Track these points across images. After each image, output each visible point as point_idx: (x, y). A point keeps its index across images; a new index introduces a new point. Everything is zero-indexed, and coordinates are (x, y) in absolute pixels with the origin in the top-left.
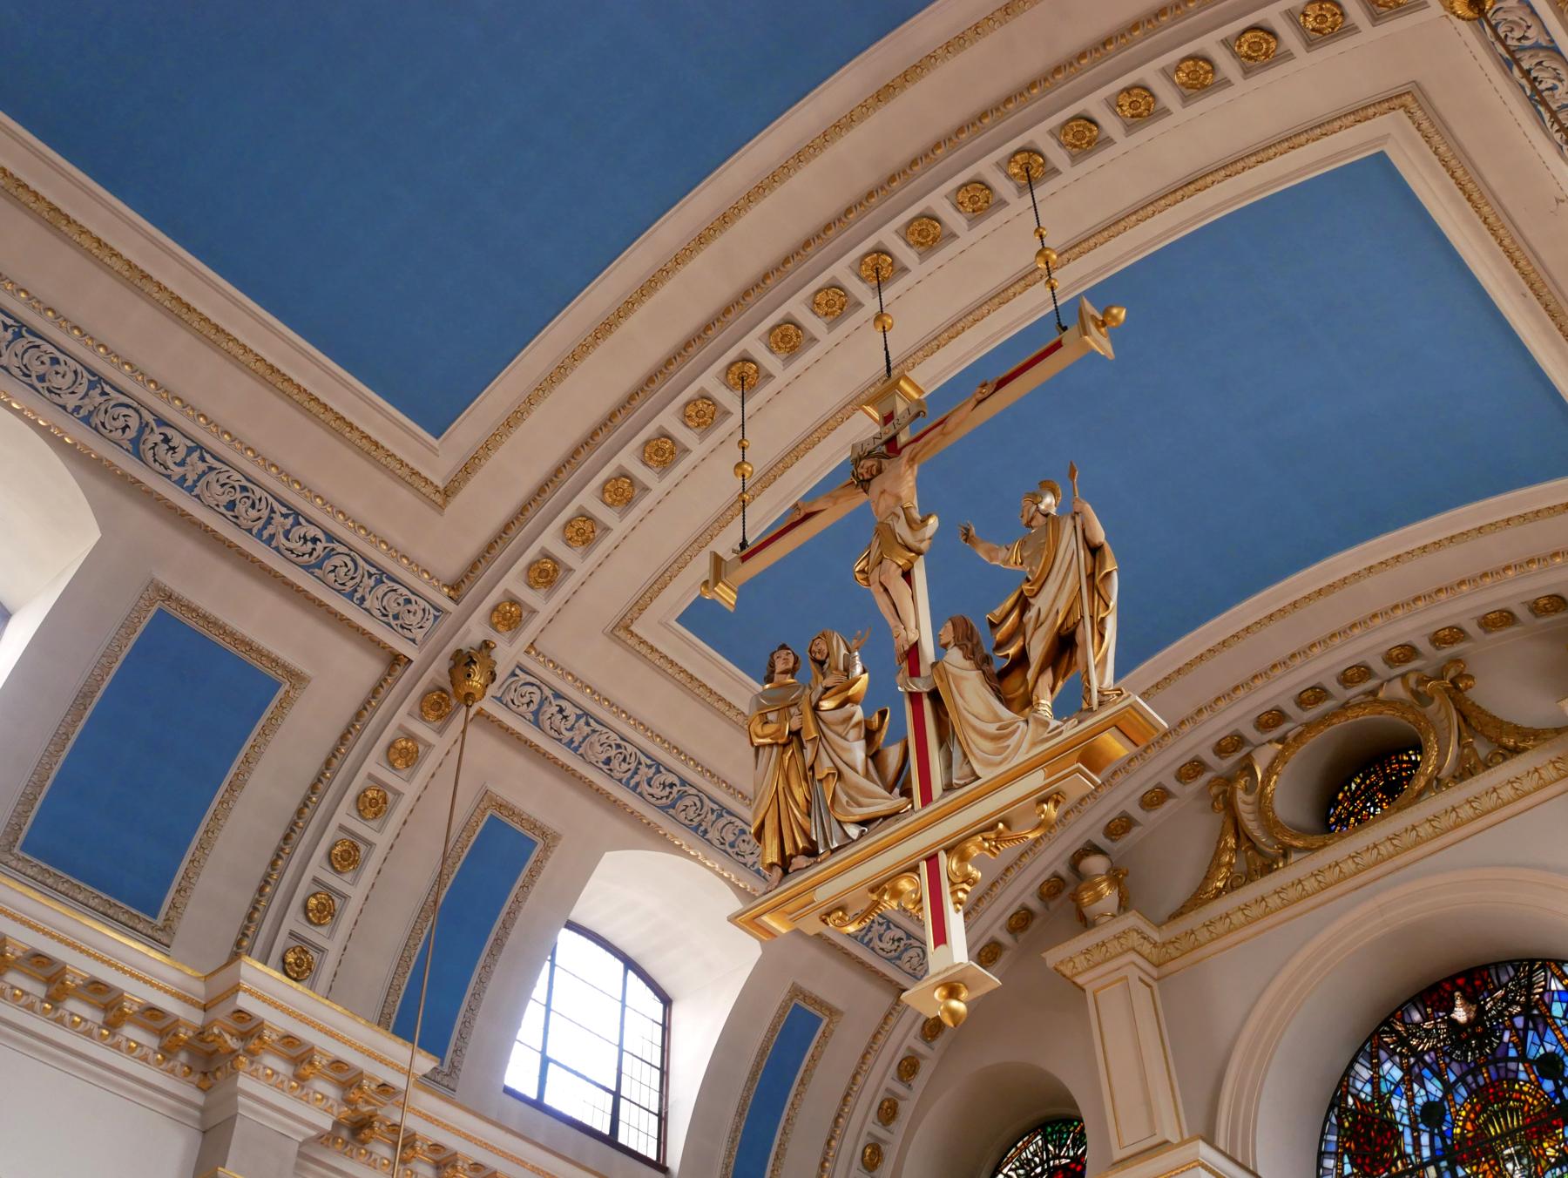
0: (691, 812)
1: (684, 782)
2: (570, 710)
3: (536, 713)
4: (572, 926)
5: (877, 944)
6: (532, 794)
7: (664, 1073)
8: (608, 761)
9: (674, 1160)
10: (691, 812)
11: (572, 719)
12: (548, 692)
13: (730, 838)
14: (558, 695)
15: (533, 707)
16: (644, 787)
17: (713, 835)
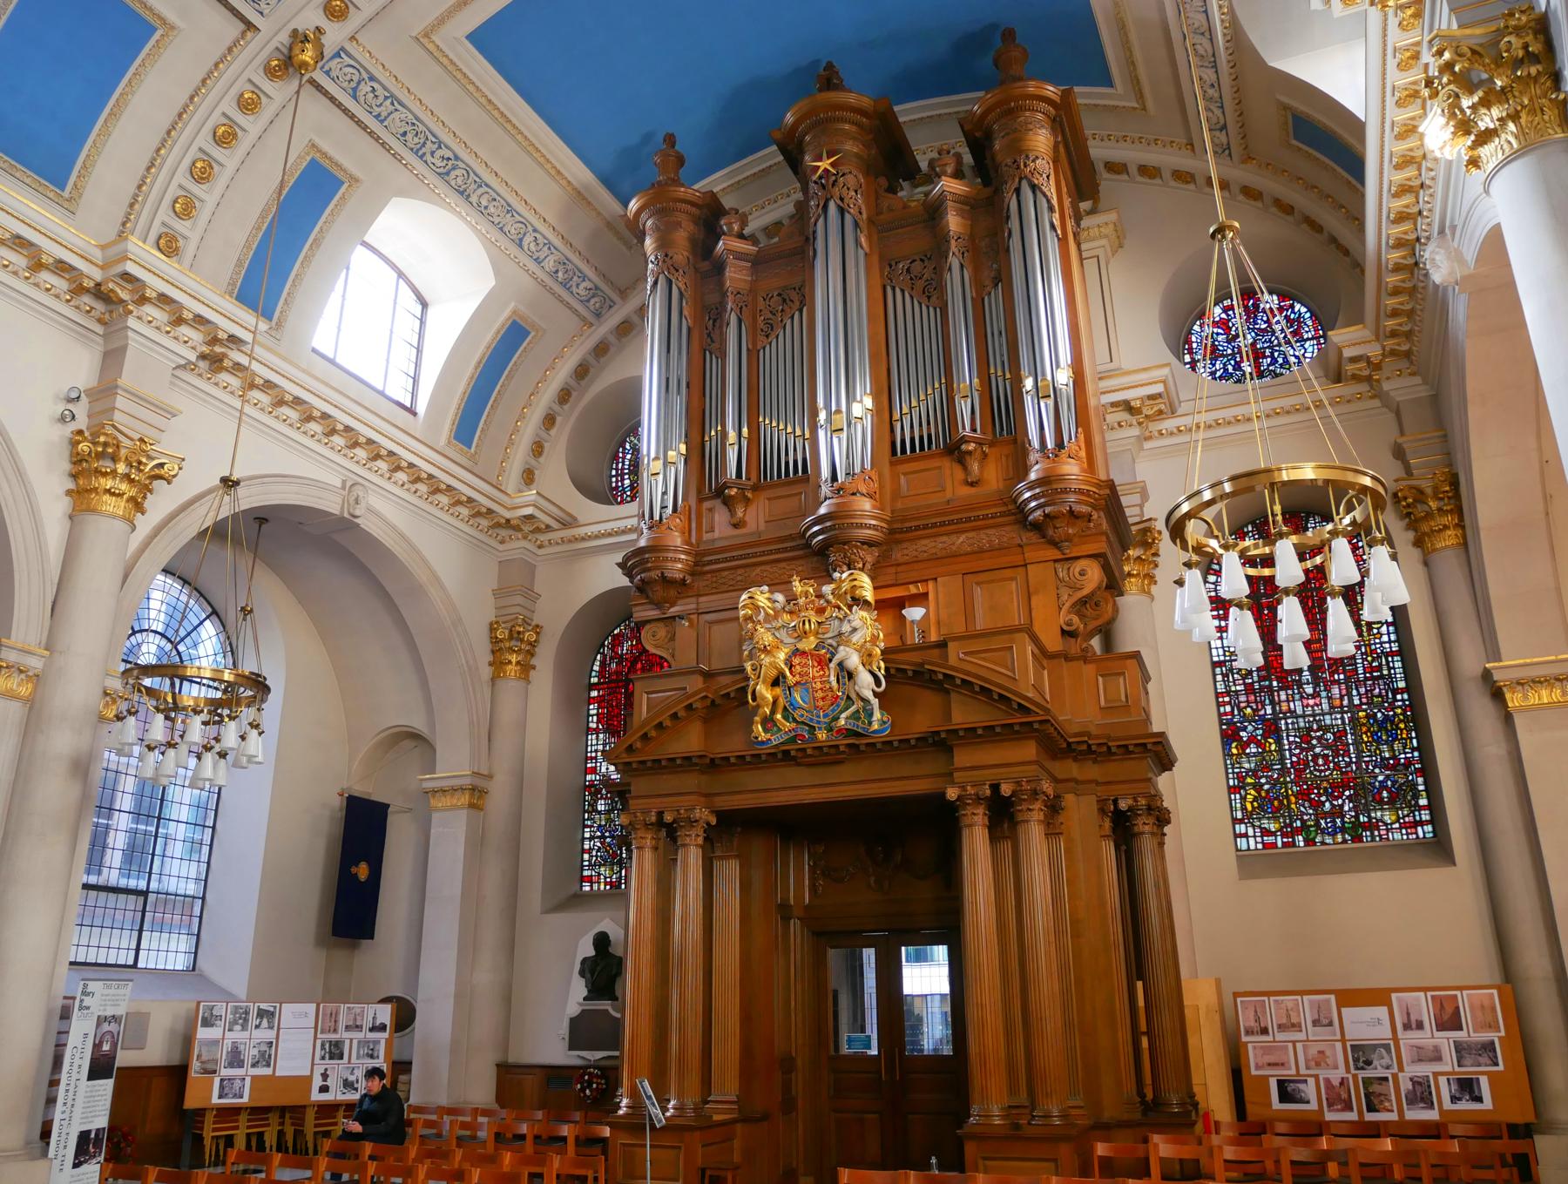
0: (459, 180)
1: (457, 158)
2: (380, 92)
3: (355, 90)
4: (365, 244)
5: (574, 289)
6: (346, 148)
7: (419, 350)
8: (405, 134)
9: (421, 407)
10: (459, 180)
11: (381, 99)
12: (365, 76)
13: (484, 203)
14: (372, 78)
15: (353, 85)
16: (428, 157)
17: (474, 199)
